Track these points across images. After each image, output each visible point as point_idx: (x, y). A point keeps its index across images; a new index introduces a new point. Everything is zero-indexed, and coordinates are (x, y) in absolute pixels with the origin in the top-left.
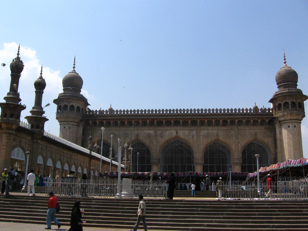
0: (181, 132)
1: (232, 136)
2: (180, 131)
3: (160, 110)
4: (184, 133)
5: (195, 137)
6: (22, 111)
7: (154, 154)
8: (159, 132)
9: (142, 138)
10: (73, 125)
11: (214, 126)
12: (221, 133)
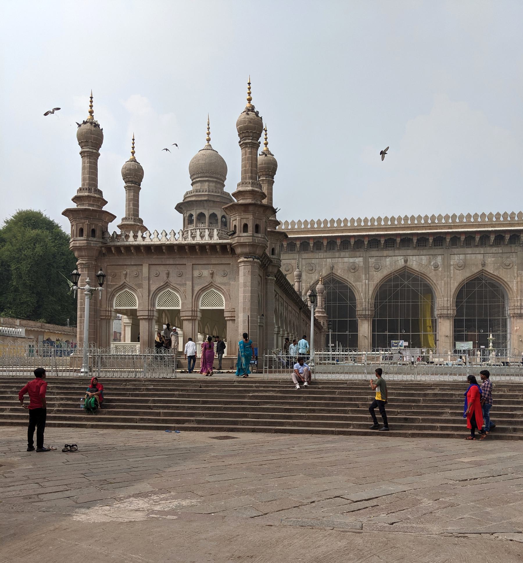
0: (414, 258)
1: (511, 266)
2: (411, 257)
3: (374, 219)
4: (418, 261)
5: (440, 269)
6: (110, 224)
7: (363, 300)
8: (372, 261)
11: (477, 246)
12: (490, 260)
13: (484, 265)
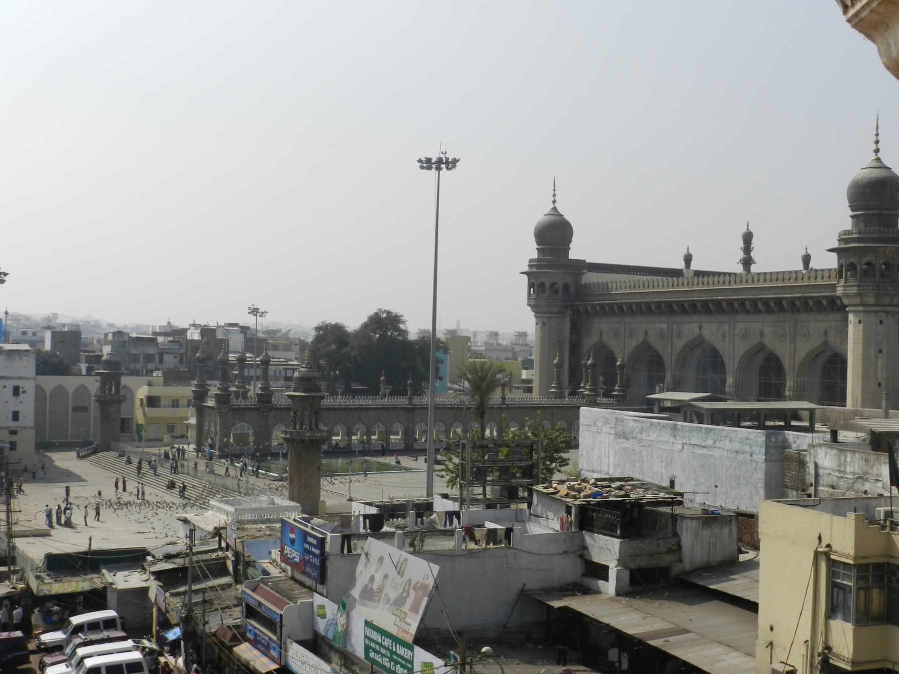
4: (711, 330)
5: (727, 339)
10: (549, 317)
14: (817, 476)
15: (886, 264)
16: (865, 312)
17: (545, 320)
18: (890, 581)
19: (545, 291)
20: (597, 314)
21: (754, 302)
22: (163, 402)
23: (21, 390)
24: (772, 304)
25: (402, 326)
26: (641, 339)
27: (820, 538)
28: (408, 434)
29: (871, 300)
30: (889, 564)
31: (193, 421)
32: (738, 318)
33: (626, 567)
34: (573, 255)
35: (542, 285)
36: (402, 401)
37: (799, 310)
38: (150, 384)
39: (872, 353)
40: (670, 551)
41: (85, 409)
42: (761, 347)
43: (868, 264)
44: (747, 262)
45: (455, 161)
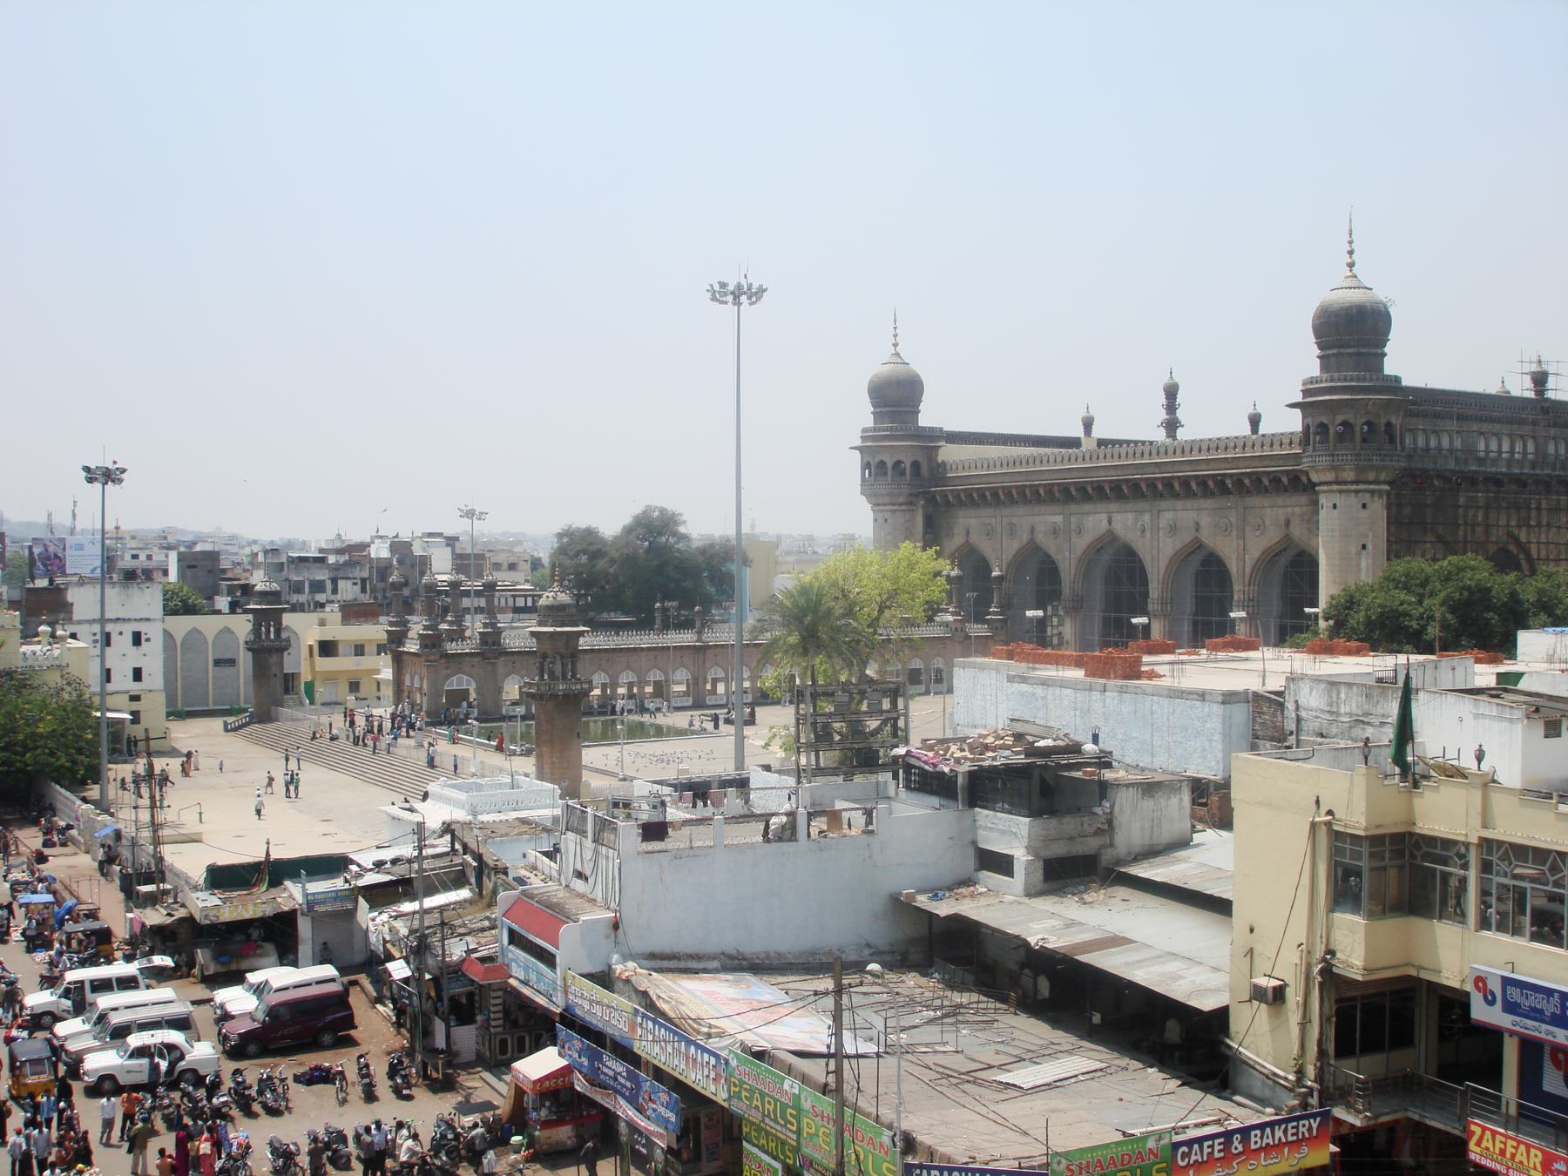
4: (1126, 522)
5: (1148, 535)
8: (1073, 519)
9: (1041, 538)
12: (1206, 520)
13: (1197, 527)
14: (1299, 720)
15: (1368, 423)
16: (1340, 492)
17: (887, 515)
18: (1412, 856)
19: (886, 474)
20: (961, 504)
21: (1185, 482)
22: (341, 648)
23: (143, 637)
24: (1211, 483)
25: (682, 529)
26: (1025, 538)
27: (1318, 802)
28: (695, 684)
29: (1349, 475)
30: (1411, 834)
31: (387, 674)
32: (1163, 504)
33: (1037, 856)
34: (928, 417)
35: (882, 464)
36: (687, 638)
37: (1248, 492)
38: (322, 623)
39: (1353, 549)
40: (1099, 832)
41: (232, 662)
42: (1197, 545)
43: (1345, 424)
44: (1172, 426)
45: (762, 290)
